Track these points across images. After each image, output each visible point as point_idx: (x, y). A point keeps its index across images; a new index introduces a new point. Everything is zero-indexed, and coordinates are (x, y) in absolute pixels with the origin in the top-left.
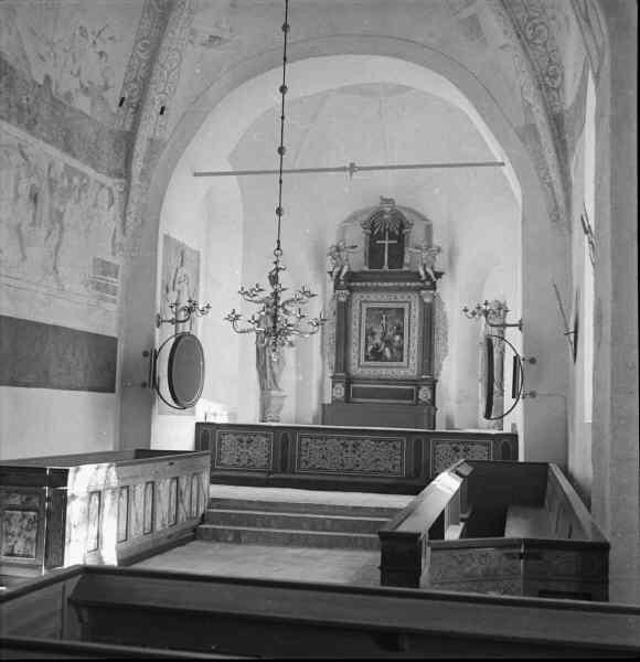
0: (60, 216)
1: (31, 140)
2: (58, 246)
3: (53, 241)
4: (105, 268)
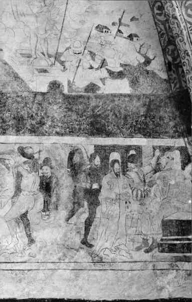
0: (93, 196)
1: (34, 139)
2: (88, 224)
3: (83, 215)
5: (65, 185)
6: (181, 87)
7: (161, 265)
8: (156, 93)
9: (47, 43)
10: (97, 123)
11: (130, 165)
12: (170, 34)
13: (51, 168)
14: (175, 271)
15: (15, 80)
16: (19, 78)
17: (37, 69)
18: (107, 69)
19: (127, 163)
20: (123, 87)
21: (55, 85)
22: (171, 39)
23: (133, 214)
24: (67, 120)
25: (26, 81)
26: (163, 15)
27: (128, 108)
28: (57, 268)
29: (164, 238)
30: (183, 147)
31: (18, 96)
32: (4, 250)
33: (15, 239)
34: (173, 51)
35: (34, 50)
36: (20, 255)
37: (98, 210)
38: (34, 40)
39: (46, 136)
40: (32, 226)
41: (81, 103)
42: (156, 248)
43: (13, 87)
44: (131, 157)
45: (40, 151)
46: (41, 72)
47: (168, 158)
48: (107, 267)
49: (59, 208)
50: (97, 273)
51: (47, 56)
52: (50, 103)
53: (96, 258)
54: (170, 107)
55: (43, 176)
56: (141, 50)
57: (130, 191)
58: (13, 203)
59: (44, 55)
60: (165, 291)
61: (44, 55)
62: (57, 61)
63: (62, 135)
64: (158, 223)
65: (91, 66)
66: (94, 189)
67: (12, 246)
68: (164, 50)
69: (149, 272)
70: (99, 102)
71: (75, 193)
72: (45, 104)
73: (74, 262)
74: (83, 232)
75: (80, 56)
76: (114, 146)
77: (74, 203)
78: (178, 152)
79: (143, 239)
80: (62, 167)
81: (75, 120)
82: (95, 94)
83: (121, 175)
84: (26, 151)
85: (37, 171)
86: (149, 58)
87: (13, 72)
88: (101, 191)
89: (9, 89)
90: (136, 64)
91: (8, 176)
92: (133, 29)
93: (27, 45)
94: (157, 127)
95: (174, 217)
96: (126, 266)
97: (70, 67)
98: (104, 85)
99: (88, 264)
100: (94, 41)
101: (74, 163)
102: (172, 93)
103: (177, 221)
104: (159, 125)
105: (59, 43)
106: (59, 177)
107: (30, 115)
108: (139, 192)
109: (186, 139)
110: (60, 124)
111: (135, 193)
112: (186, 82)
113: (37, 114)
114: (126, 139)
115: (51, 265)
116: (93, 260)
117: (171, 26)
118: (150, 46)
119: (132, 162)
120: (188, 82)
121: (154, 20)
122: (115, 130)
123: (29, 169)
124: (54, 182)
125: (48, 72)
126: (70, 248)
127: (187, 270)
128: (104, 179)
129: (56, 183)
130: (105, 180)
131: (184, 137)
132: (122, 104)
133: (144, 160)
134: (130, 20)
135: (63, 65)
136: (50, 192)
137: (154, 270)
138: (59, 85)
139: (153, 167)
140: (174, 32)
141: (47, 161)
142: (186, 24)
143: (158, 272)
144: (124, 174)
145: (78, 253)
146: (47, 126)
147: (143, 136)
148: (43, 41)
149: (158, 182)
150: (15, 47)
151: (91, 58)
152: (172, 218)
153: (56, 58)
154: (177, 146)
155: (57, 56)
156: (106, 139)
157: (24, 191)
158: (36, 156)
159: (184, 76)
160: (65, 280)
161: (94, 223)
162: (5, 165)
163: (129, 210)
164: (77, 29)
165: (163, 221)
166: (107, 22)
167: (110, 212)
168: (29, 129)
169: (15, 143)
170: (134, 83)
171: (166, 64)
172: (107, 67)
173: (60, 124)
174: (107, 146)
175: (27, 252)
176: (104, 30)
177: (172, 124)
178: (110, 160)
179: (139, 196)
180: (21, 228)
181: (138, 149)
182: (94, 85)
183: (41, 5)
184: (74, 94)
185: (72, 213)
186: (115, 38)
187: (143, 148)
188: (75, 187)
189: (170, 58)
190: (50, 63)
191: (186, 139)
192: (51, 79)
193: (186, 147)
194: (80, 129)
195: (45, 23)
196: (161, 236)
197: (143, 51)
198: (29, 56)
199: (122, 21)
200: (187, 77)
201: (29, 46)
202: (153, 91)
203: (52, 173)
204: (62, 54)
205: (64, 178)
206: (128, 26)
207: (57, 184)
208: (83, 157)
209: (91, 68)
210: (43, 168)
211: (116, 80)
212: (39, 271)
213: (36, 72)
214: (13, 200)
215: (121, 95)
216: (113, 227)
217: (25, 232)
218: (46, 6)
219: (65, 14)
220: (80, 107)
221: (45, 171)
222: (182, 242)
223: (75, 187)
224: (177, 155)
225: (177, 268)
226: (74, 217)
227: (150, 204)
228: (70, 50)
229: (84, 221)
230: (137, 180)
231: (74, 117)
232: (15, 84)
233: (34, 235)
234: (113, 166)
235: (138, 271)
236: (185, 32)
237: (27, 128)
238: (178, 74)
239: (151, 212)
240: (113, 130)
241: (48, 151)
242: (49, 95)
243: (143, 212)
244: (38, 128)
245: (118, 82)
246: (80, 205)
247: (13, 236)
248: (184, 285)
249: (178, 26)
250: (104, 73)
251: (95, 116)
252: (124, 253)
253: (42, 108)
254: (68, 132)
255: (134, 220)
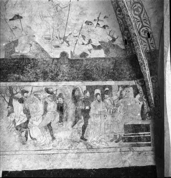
0: (86, 113)
1: (54, 83)
2: (84, 128)
4: (136, 128)
5: (70, 107)
6: (132, 53)
7: (124, 149)
8: (119, 56)
9: (59, 32)
10: (87, 74)
11: (106, 96)
12: (126, 25)
13: (63, 99)
14: (132, 152)
15: (42, 52)
16: (44, 51)
17: (54, 46)
18: (92, 45)
19: (104, 95)
20: (101, 54)
21: (64, 54)
22: (126, 27)
23: (108, 122)
24: (71, 73)
25: (48, 52)
26: (122, 14)
27: (104, 65)
28: (68, 152)
29: (125, 134)
30: (135, 85)
31: (44, 61)
32: (39, 143)
33: (45, 137)
34: (127, 34)
35: (52, 35)
36: (48, 146)
37: (90, 121)
38: (52, 30)
39: (60, 82)
40: (54, 130)
41: (78, 63)
42: (121, 140)
43: (41, 56)
44: (106, 91)
45: (56, 90)
46: (56, 47)
47: (126, 91)
48: (95, 151)
49: (68, 120)
50: (90, 154)
51: (59, 39)
52: (61, 64)
53: (89, 147)
54: (127, 64)
55: (59, 103)
56: (110, 34)
57: (106, 110)
58: (43, 118)
59: (58, 38)
60: (127, 163)
61: (58, 38)
62: (65, 41)
63: (68, 81)
64: (122, 126)
65: (83, 43)
66: (86, 109)
67: (43, 141)
68: (122, 34)
69: (118, 153)
70: (88, 62)
71: (76, 112)
72: (59, 65)
73: (77, 149)
74: (81, 133)
75: (77, 38)
76: (97, 86)
77: (76, 117)
78: (131, 88)
79: (114, 135)
80: (69, 98)
81: (75, 72)
82: (86, 58)
83: (101, 101)
84: (49, 90)
85: (55, 101)
86: (115, 38)
87: (41, 48)
88: (91, 110)
89: (39, 57)
90: (108, 41)
91: (40, 104)
92: (106, 23)
93: (48, 33)
94: (120, 74)
95: (130, 123)
96: (105, 150)
97: (72, 44)
98: (90, 53)
99: (84, 150)
100: (85, 30)
101: (75, 96)
102: (128, 57)
103: (132, 125)
104: (121, 74)
105: (65, 31)
106: (67, 104)
107: (51, 71)
108: (111, 110)
109: (136, 81)
110: (67, 75)
111: (109, 111)
112: (135, 50)
113: (54, 70)
114: (103, 82)
115: (65, 150)
116: (87, 147)
117: (126, 20)
118: (115, 31)
119: (106, 94)
120: (136, 50)
121: (117, 18)
122: (97, 77)
123: (51, 99)
124: (65, 106)
125: (60, 47)
126: (74, 142)
127: (138, 151)
128: (92, 104)
129: (66, 107)
130: (92, 105)
131: (135, 80)
132: (101, 64)
133: (113, 93)
134: (103, 18)
135: (68, 43)
136: (62, 112)
137: (120, 152)
138: (66, 54)
139: (119, 96)
140: (128, 24)
141: (60, 95)
142: (134, 19)
143: (123, 153)
144: (103, 101)
145: (79, 144)
146: (60, 76)
147: (112, 80)
148: (56, 31)
149: (121, 104)
150: (42, 34)
151: (83, 39)
152: (129, 124)
153: (64, 39)
154: (131, 85)
155: (65, 38)
156: (93, 82)
157: (49, 111)
158: (55, 93)
159: (134, 47)
160: (72, 158)
161: (87, 128)
162: (38, 98)
163: (106, 120)
164: (75, 24)
165: (125, 125)
166: (91, 19)
167: (96, 121)
168: (50, 78)
169: (43, 86)
170: (107, 51)
171: (124, 41)
172: (92, 43)
173: (67, 75)
174: (93, 86)
175: (52, 144)
176: (90, 24)
177: (128, 73)
178: (95, 93)
179: (111, 113)
180: (48, 132)
181: (110, 87)
182: (85, 53)
183: (55, 11)
184: (74, 58)
185: (75, 123)
186: (96, 27)
187: (113, 86)
188: (76, 108)
189: (126, 38)
190: (61, 42)
191: (136, 81)
192: (62, 51)
193: (136, 85)
194: (78, 77)
195: (57, 21)
196: (124, 133)
197: (111, 35)
198: (49, 39)
199: (100, 19)
200: (135, 48)
201: (49, 34)
202: (117, 56)
203: (63, 101)
204: (67, 37)
205: (70, 104)
206: (103, 21)
207: (66, 107)
208: (80, 92)
209: (83, 44)
210: (59, 99)
211: (97, 50)
212: (58, 154)
213: (53, 47)
214: (43, 116)
215: (100, 58)
216: (98, 129)
217: (50, 134)
218: (58, 12)
219: (68, 16)
220: (78, 65)
221: (59, 100)
222: (135, 136)
223: (76, 108)
224: (131, 90)
225: (133, 150)
226: (76, 125)
227: (117, 117)
228: (71, 35)
229: (81, 127)
230: (110, 104)
231: (75, 71)
232: (42, 54)
233: (55, 135)
234: (96, 97)
235: (112, 153)
236: (134, 24)
237: (49, 78)
238: (130, 46)
239: (118, 120)
240: (96, 77)
241: (61, 90)
242: (60, 59)
243: (114, 121)
244: (55, 77)
245: (98, 51)
246: (79, 118)
247: (43, 136)
248: (137, 159)
249: (130, 21)
250: (90, 47)
251: (86, 70)
252: (104, 143)
253: (57, 66)
254: (71, 79)
255: (109, 125)
